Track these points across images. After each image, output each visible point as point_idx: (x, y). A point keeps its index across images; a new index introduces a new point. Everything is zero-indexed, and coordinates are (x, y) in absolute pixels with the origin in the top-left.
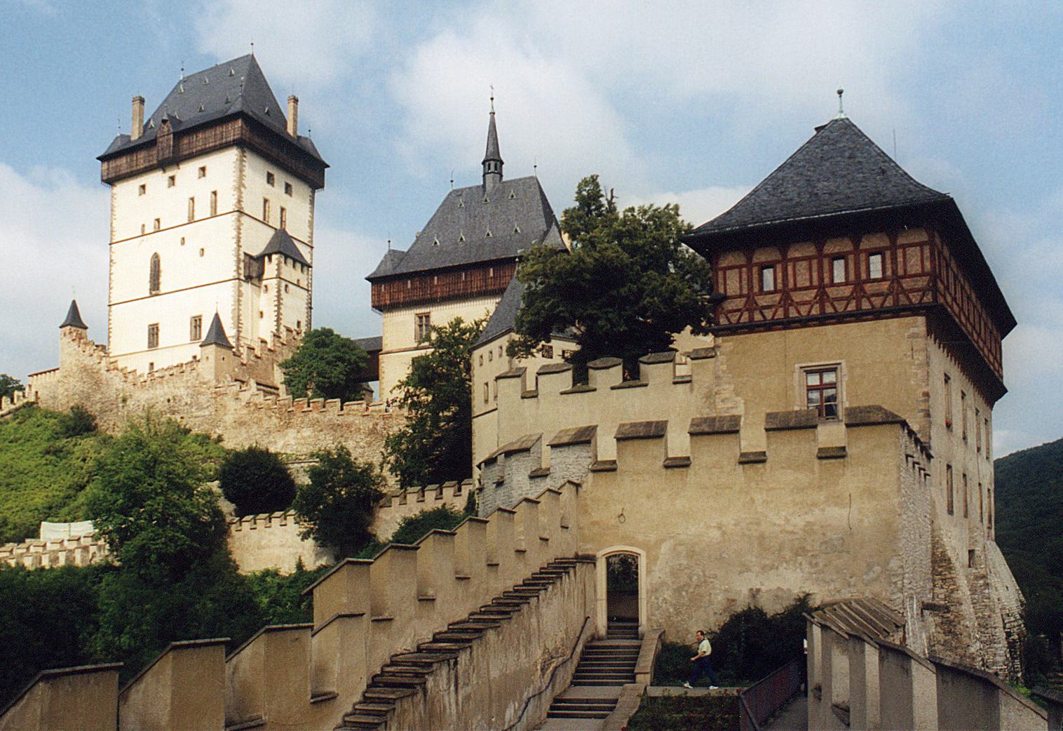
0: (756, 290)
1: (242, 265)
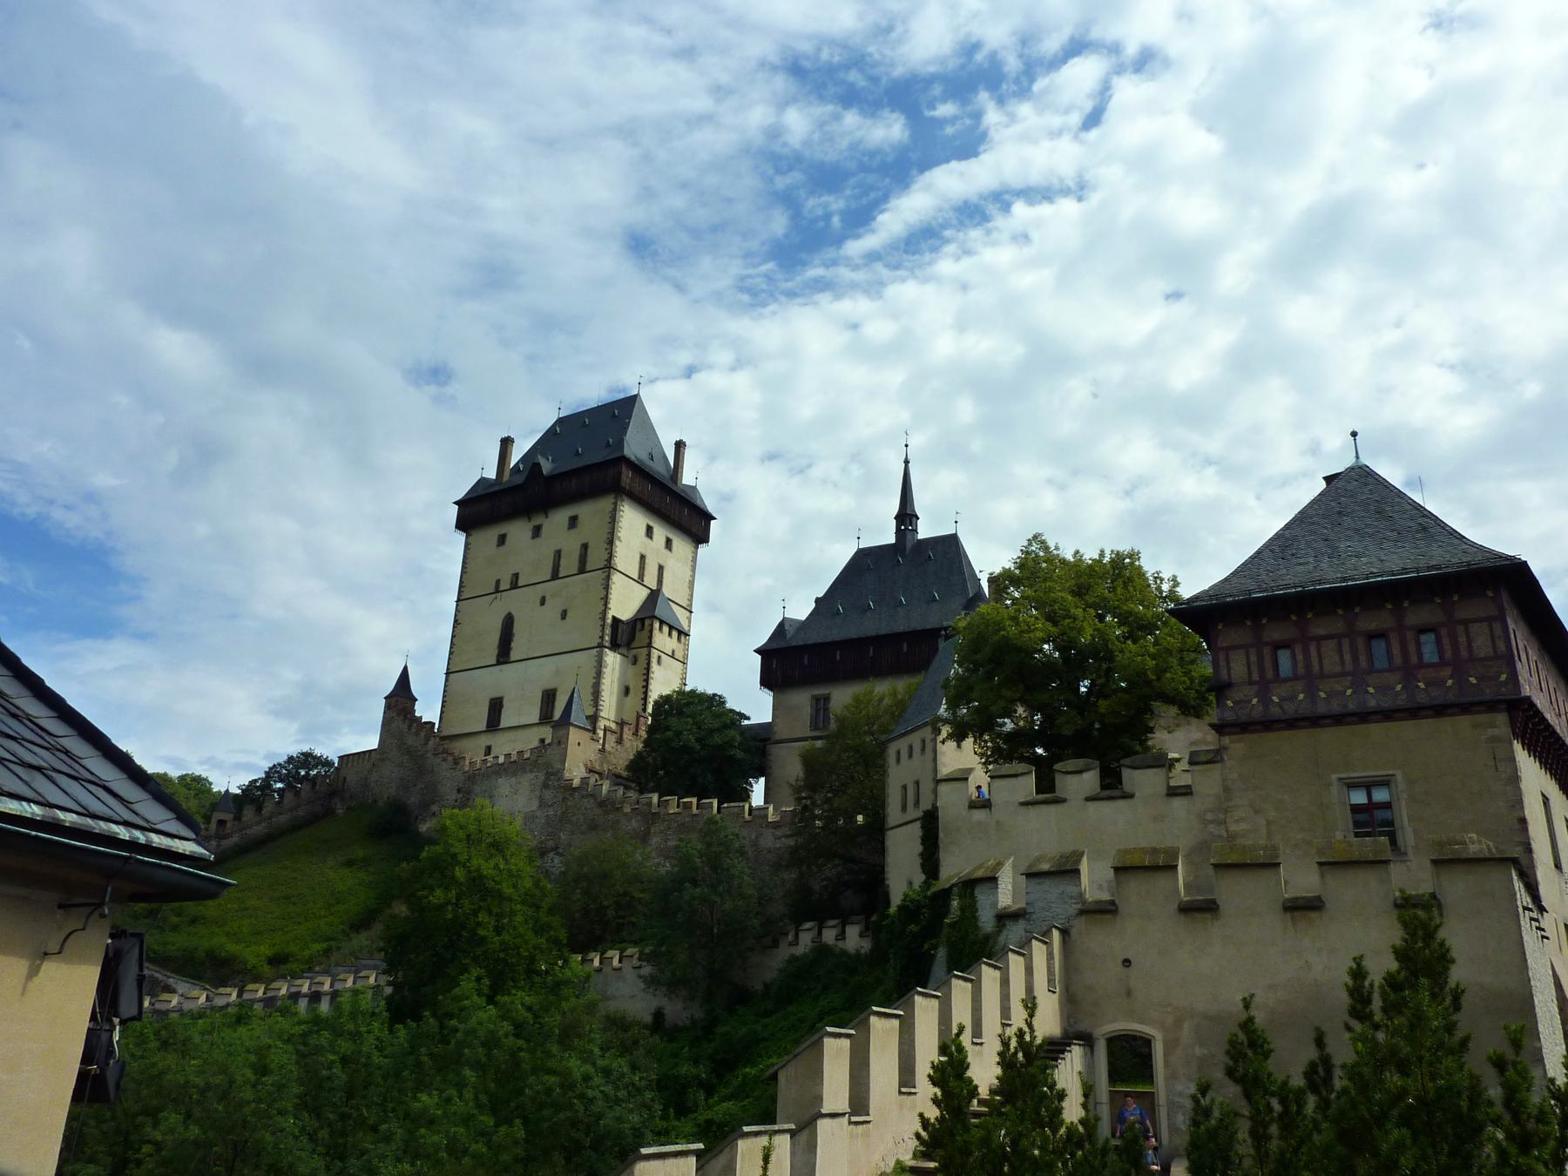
0: (1270, 674)
1: (608, 631)
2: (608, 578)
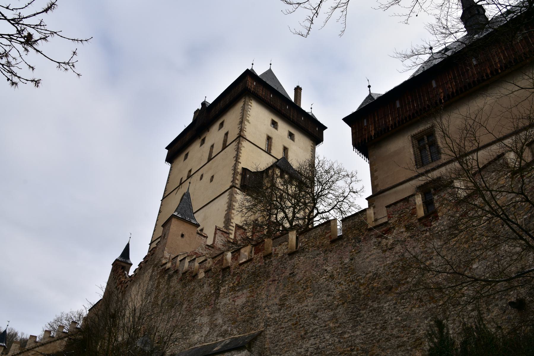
1: (239, 177)
2: (239, 143)
